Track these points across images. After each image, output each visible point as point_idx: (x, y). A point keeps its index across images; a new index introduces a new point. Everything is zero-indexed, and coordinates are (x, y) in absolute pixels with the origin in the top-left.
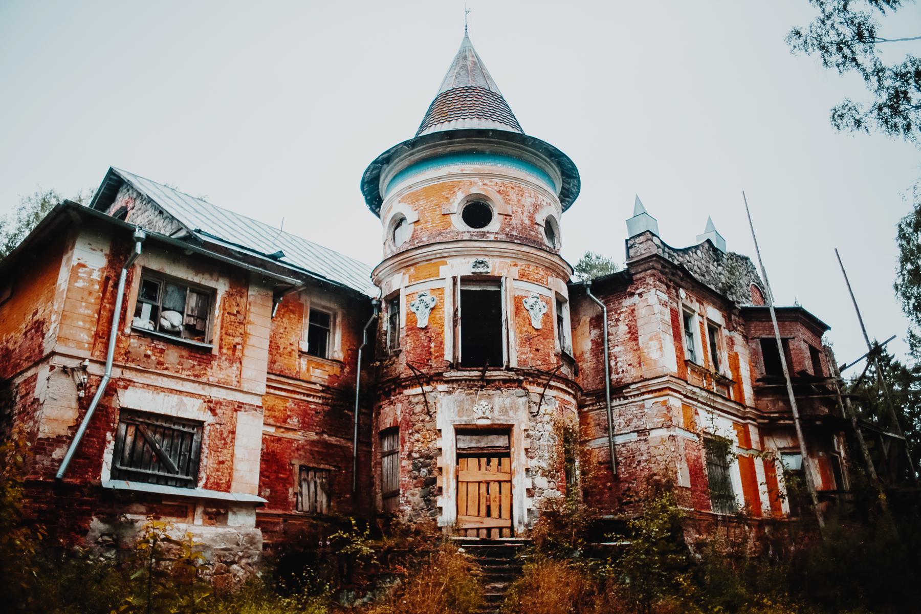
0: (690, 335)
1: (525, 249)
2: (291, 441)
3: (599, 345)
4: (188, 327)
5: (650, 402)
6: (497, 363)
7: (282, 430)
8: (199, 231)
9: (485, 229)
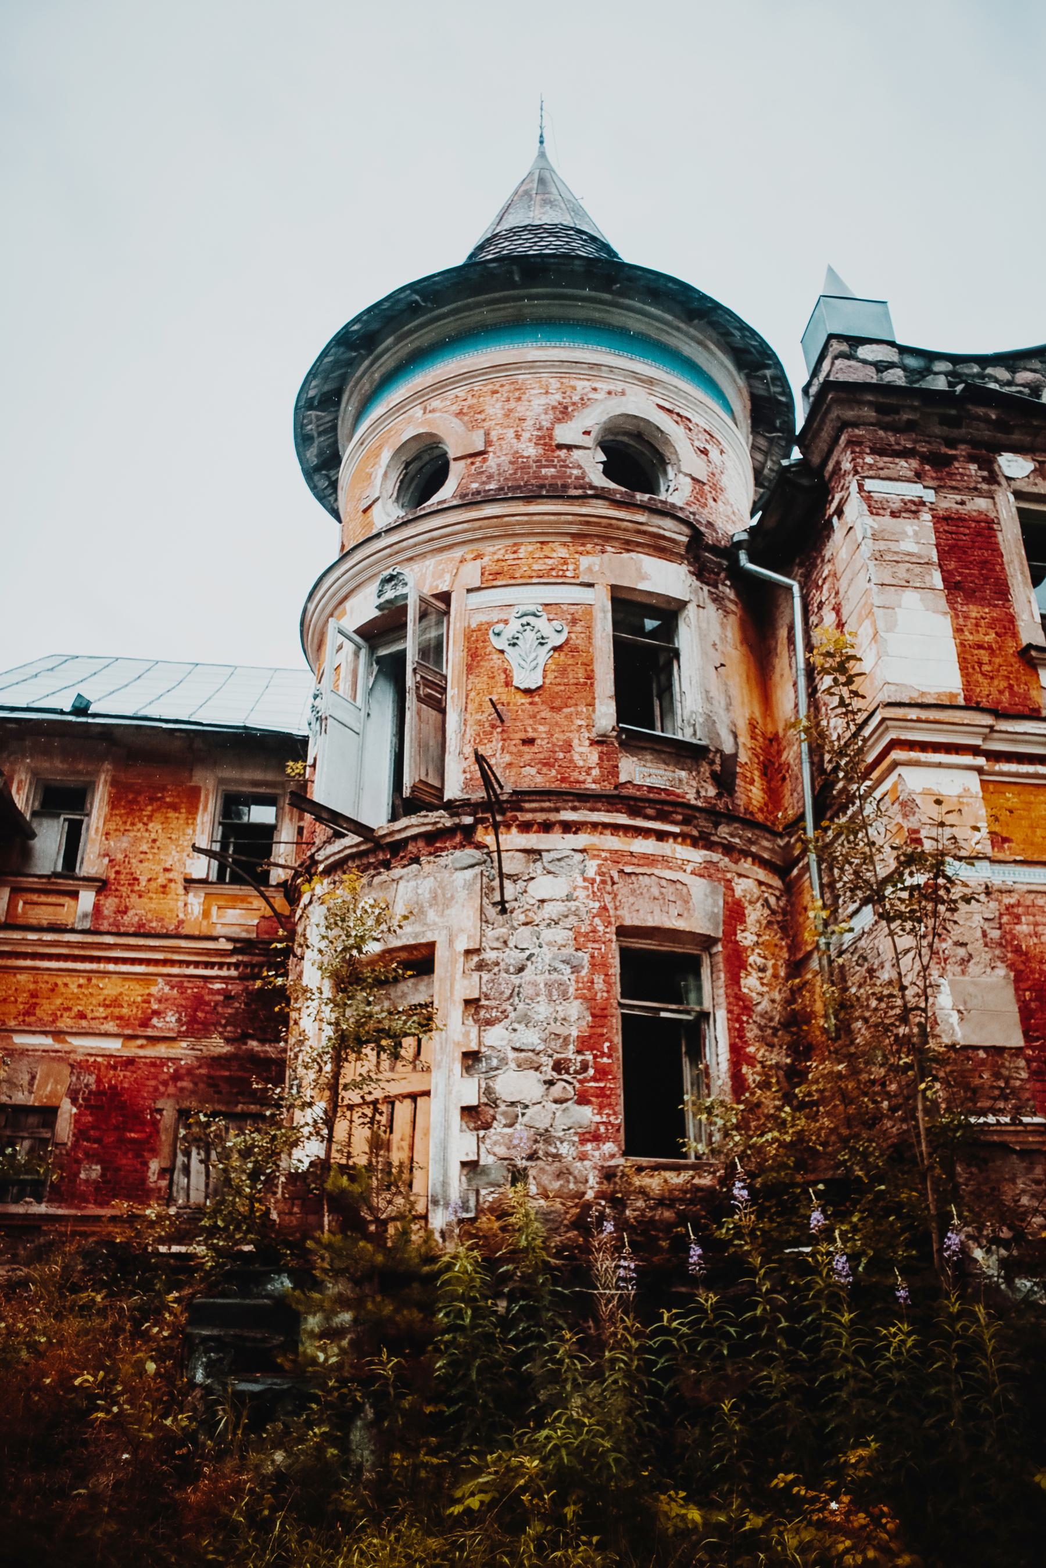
2: (158, 1063)
7: (140, 1042)
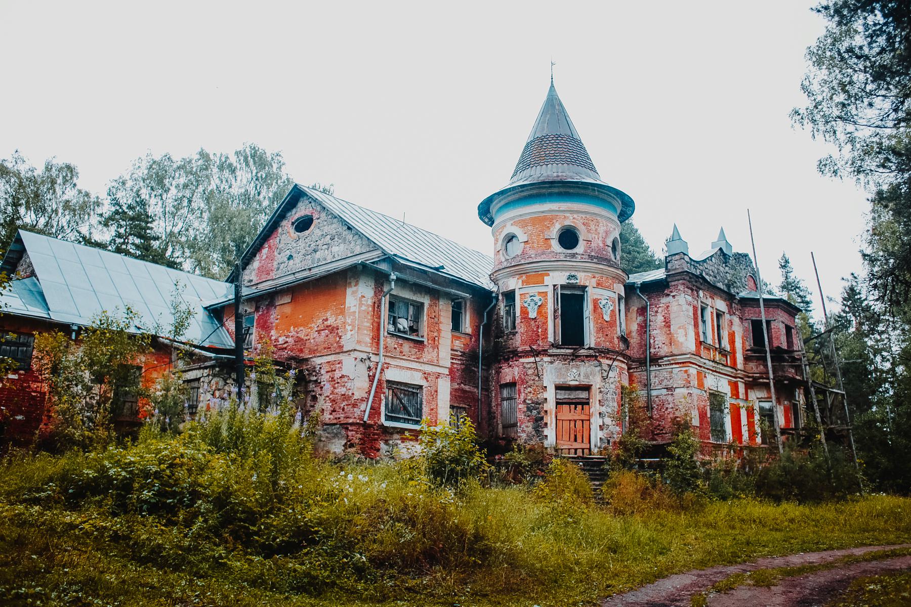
0: (704, 322)
1: (601, 266)
3: (644, 328)
4: (411, 328)
5: (676, 369)
6: (581, 343)
8: (395, 255)
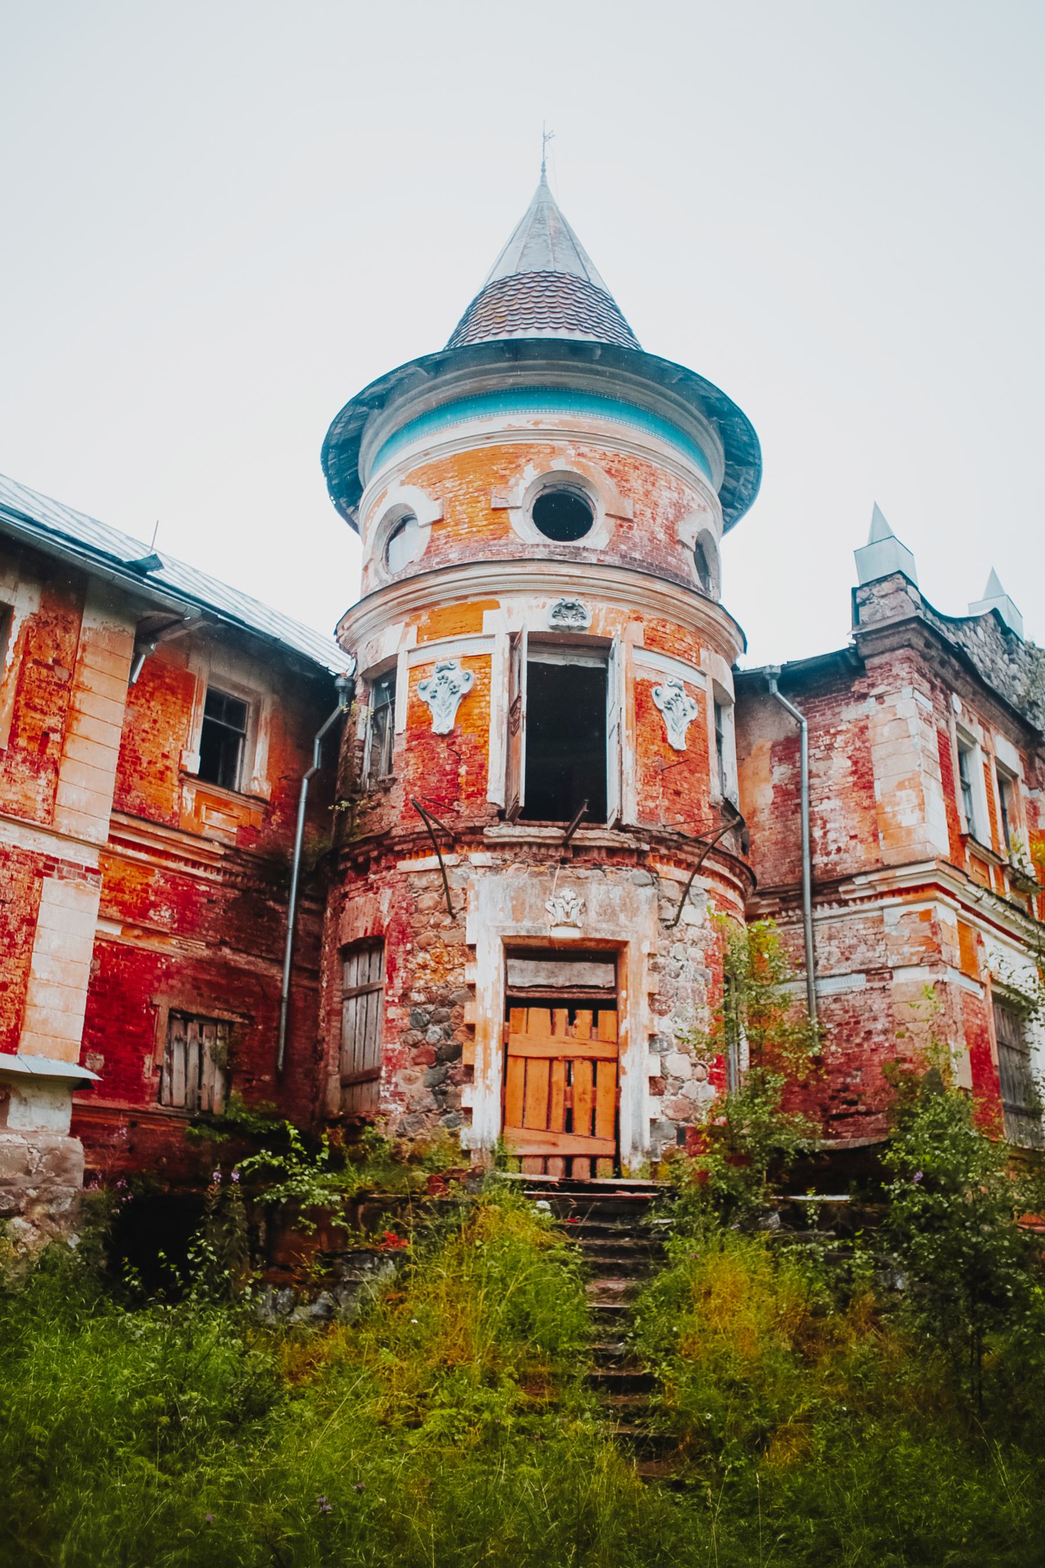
0: (966, 788)
2: (154, 958)
3: (790, 796)
5: (896, 912)
6: (598, 815)
7: (137, 932)
9: (580, 543)
